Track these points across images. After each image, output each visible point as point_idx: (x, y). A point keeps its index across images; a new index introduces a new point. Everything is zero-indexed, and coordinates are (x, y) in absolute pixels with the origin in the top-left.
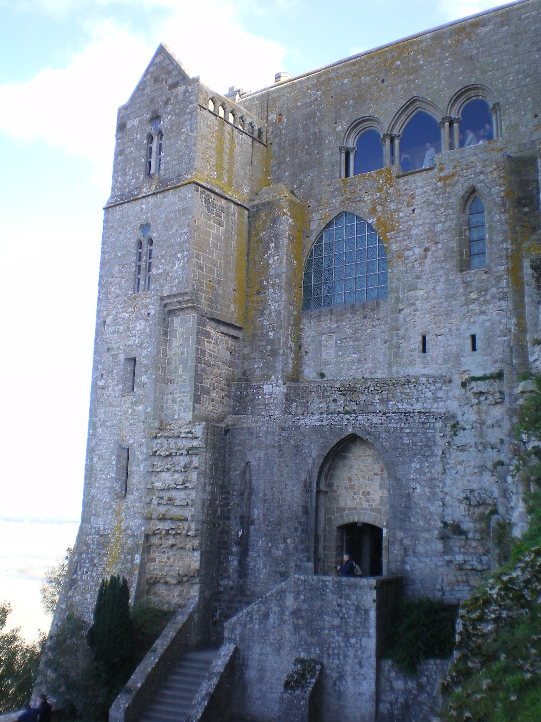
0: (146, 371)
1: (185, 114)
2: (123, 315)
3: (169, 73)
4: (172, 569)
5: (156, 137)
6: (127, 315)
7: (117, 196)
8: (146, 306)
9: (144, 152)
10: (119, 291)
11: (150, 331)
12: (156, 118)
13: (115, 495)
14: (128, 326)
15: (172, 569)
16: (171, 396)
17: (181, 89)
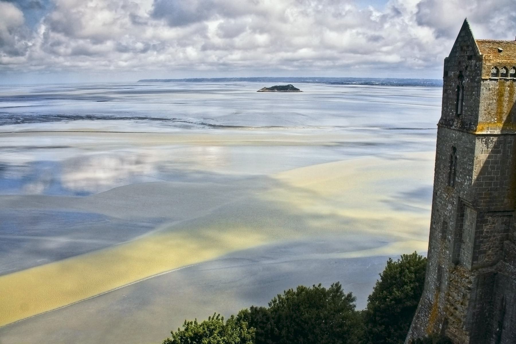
0: (451, 234)
1: (475, 81)
2: (444, 195)
3: (468, 46)
4: (455, 339)
5: (462, 89)
6: (445, 196)
7: (444, 120)
8: (453, 197)
9: (455, 97)
10: (442, 180)
11: (454, 212)
12: (461, 77)
13: (436, 287)
14: (445, 203)
15: (455, 339)
16: (463, 250)
17: (473, 62)
